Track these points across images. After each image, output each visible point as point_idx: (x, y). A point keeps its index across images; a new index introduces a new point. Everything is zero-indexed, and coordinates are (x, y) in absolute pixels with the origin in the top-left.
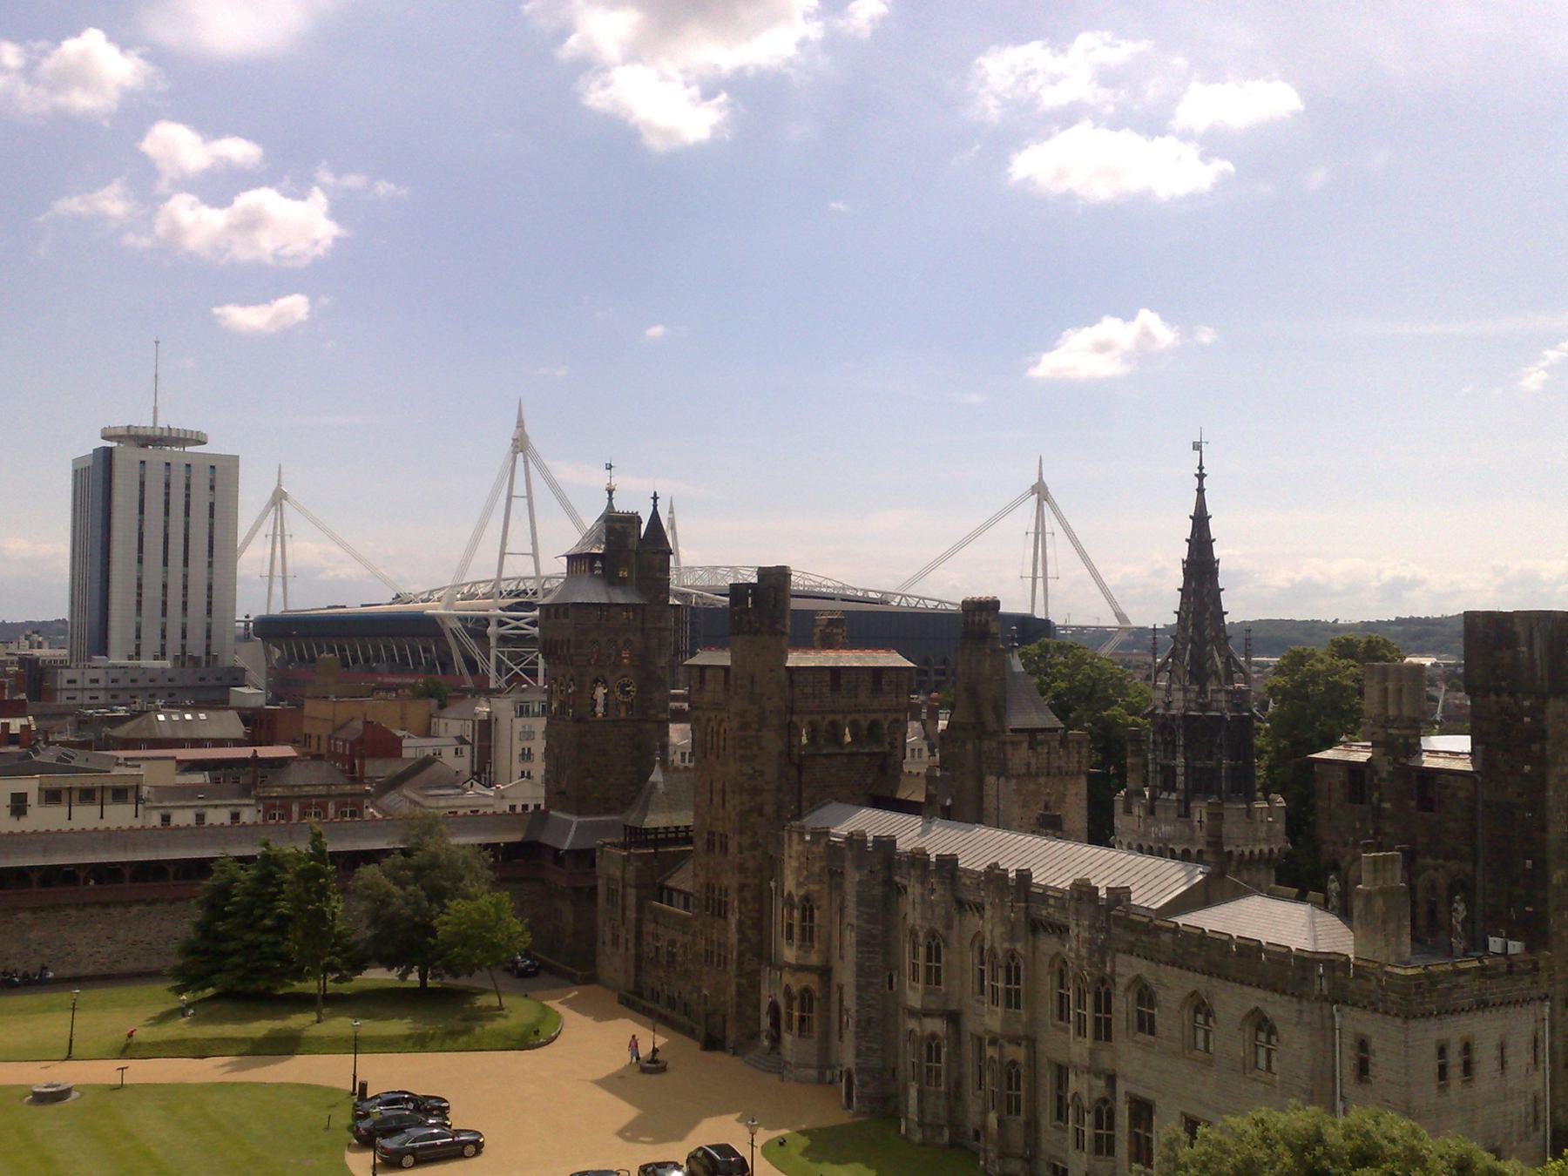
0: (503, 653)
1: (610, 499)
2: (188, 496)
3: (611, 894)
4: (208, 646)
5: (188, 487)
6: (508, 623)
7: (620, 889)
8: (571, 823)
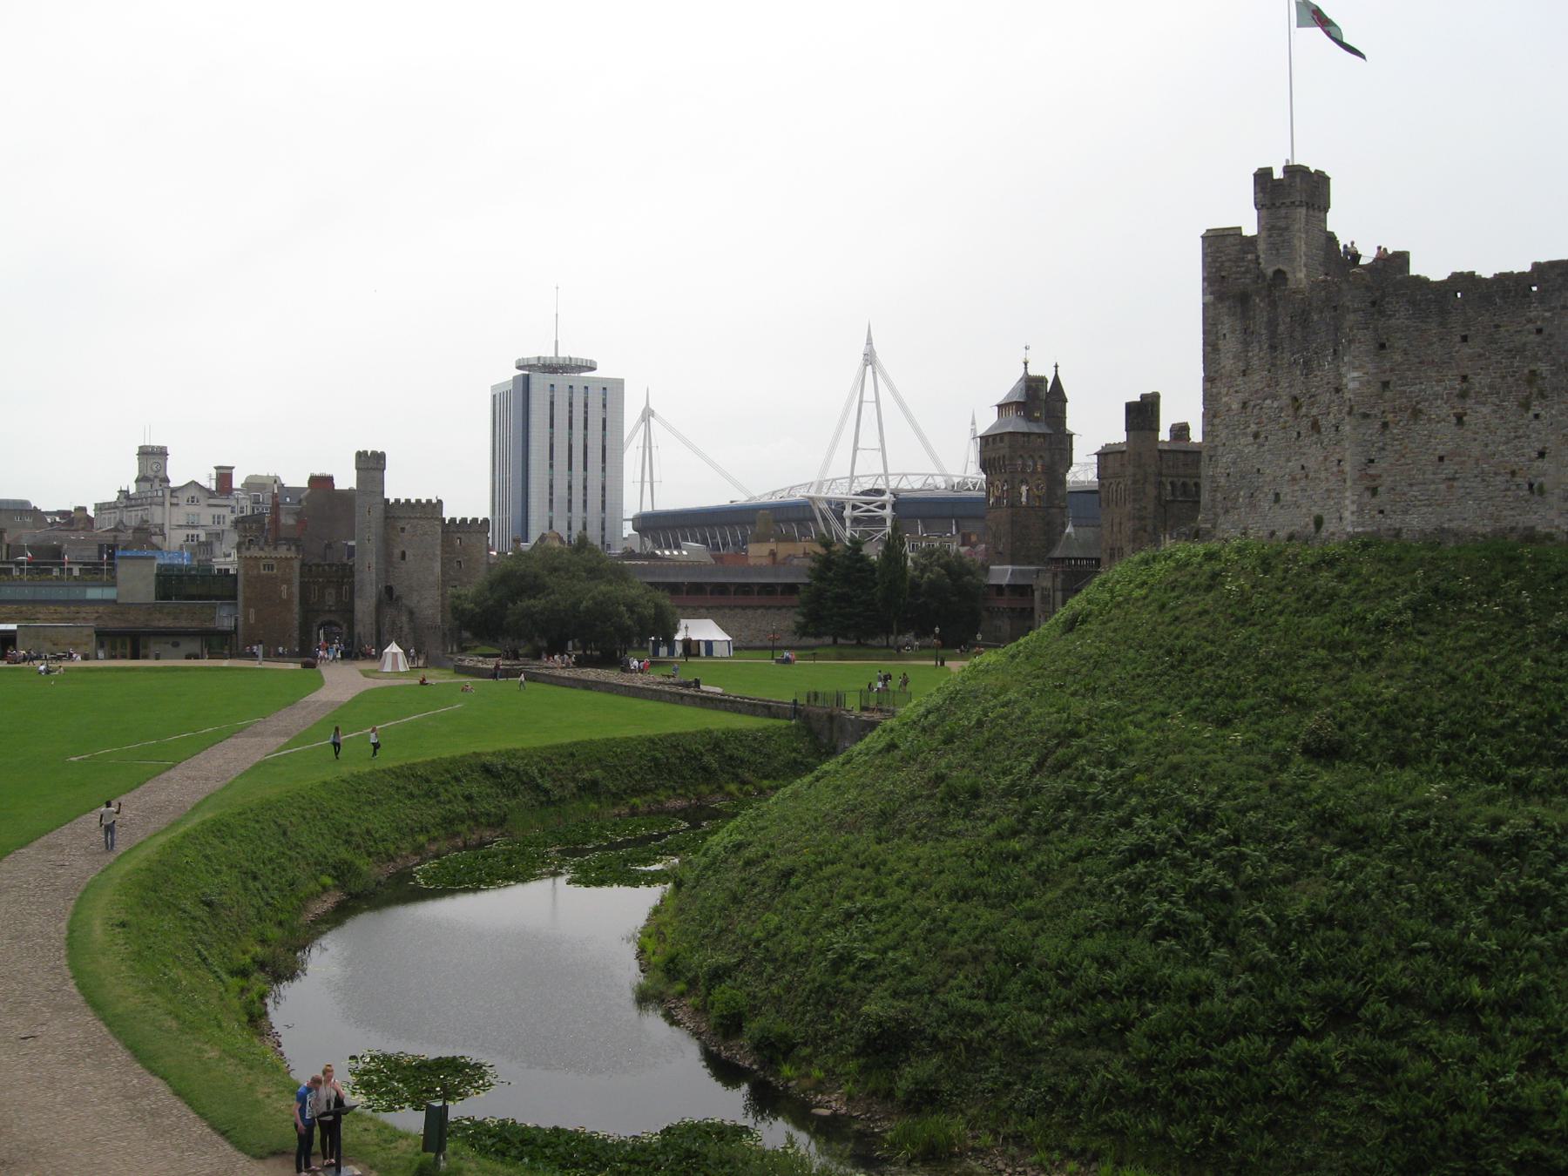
0: (856, 532)
1: (1026, 368)
2: (586, 412)
3: (1045, 599)
4: (603, 537)
5: (586, 405)
6: (860, 507)
7: (1051, 593)
8: (1007, 570)
